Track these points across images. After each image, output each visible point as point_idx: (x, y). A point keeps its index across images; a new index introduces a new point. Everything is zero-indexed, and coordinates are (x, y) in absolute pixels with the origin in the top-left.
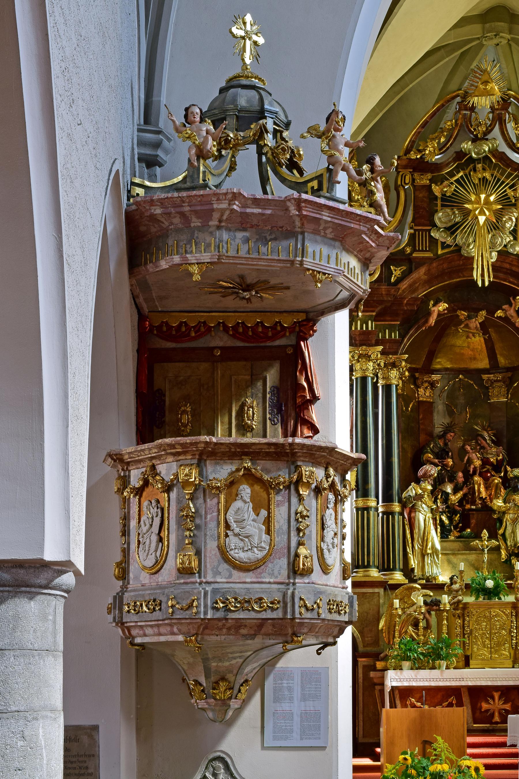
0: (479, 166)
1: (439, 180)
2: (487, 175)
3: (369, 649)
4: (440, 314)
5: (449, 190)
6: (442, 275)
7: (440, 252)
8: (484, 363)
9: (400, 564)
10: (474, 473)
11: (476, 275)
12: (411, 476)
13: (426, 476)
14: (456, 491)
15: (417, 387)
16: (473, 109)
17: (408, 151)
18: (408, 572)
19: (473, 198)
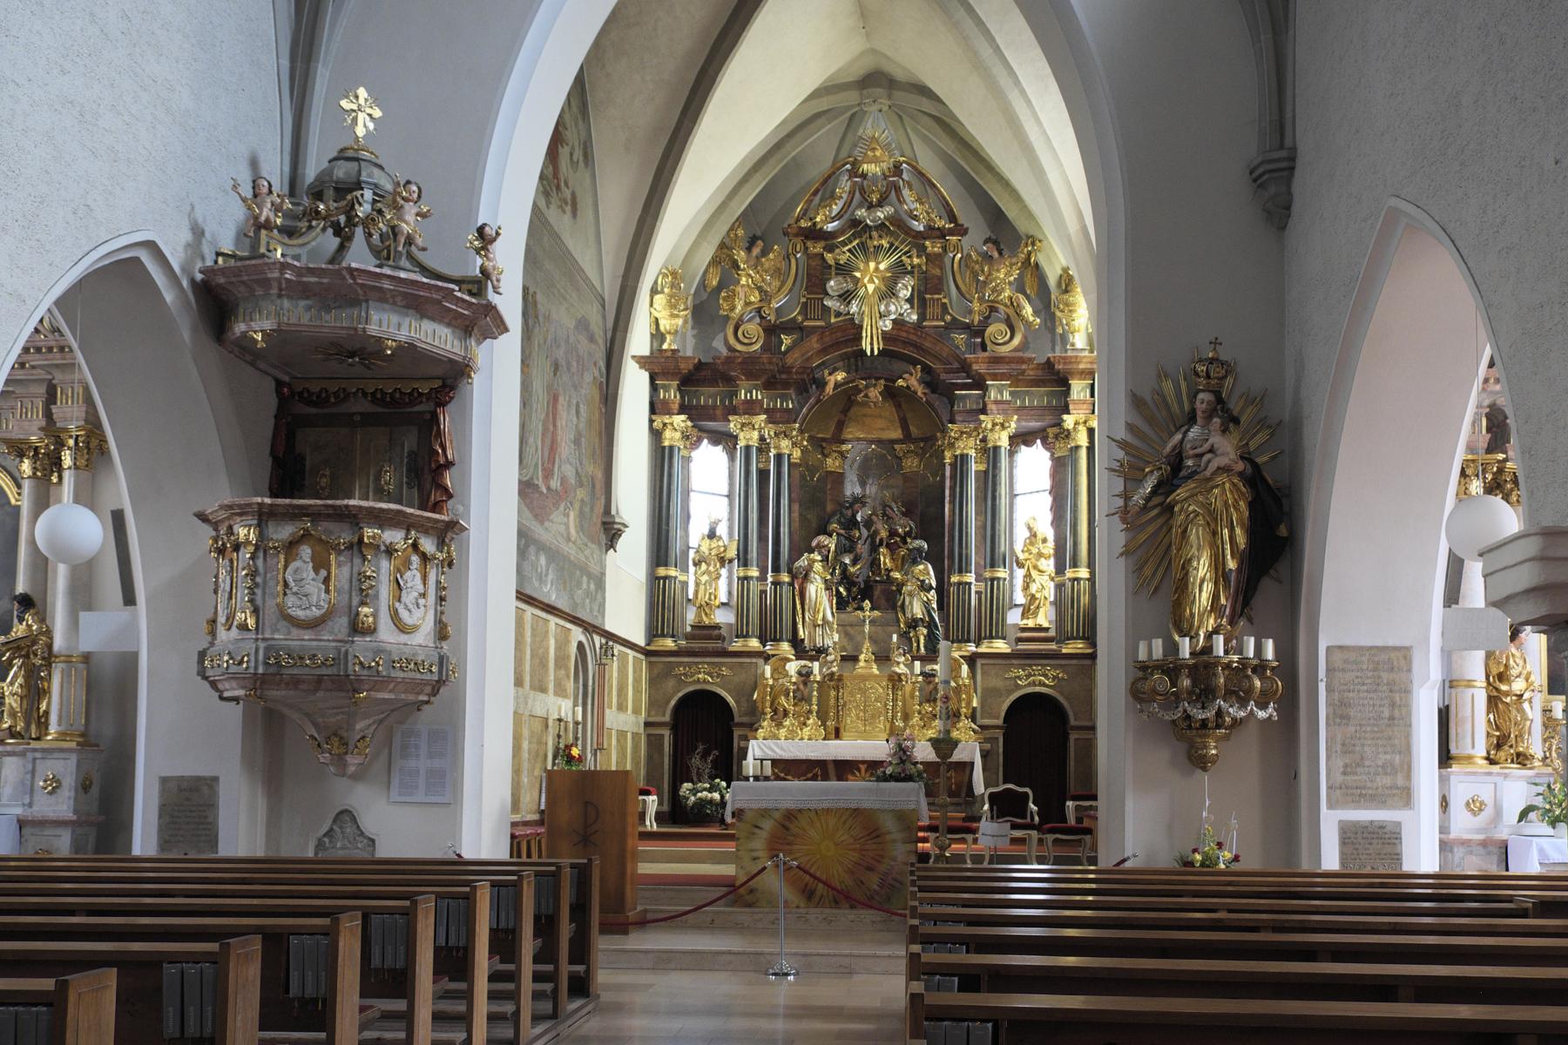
0: (874, 234)
1: (830, 249)
2: (885, 243)
3: (745, 719)
4: (837, 385)
5: (843, 259)
6: (837, 345)
7: (833, 320)
8: (896, 434)
9: (787, 633)
10: (881, 544)
11: (866, 345)
12: (802, 546)
13: (820, 547)
14: (854, 562)
15: (825, 456)
16: (864, 176)
17: (798, 220)
18: (796, 643)
19: (862, 266)
